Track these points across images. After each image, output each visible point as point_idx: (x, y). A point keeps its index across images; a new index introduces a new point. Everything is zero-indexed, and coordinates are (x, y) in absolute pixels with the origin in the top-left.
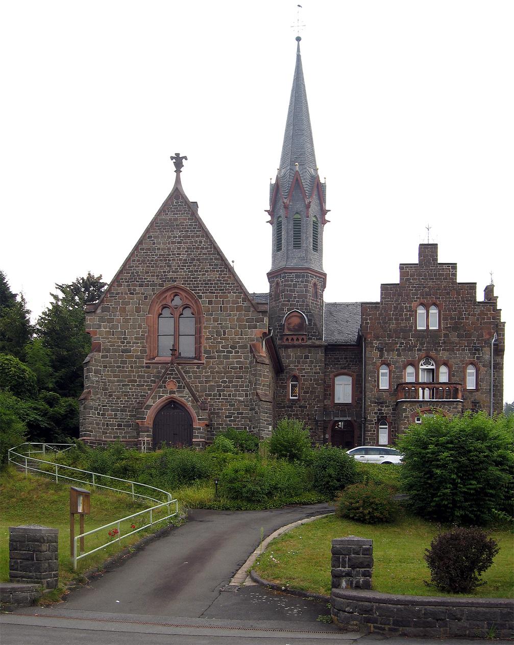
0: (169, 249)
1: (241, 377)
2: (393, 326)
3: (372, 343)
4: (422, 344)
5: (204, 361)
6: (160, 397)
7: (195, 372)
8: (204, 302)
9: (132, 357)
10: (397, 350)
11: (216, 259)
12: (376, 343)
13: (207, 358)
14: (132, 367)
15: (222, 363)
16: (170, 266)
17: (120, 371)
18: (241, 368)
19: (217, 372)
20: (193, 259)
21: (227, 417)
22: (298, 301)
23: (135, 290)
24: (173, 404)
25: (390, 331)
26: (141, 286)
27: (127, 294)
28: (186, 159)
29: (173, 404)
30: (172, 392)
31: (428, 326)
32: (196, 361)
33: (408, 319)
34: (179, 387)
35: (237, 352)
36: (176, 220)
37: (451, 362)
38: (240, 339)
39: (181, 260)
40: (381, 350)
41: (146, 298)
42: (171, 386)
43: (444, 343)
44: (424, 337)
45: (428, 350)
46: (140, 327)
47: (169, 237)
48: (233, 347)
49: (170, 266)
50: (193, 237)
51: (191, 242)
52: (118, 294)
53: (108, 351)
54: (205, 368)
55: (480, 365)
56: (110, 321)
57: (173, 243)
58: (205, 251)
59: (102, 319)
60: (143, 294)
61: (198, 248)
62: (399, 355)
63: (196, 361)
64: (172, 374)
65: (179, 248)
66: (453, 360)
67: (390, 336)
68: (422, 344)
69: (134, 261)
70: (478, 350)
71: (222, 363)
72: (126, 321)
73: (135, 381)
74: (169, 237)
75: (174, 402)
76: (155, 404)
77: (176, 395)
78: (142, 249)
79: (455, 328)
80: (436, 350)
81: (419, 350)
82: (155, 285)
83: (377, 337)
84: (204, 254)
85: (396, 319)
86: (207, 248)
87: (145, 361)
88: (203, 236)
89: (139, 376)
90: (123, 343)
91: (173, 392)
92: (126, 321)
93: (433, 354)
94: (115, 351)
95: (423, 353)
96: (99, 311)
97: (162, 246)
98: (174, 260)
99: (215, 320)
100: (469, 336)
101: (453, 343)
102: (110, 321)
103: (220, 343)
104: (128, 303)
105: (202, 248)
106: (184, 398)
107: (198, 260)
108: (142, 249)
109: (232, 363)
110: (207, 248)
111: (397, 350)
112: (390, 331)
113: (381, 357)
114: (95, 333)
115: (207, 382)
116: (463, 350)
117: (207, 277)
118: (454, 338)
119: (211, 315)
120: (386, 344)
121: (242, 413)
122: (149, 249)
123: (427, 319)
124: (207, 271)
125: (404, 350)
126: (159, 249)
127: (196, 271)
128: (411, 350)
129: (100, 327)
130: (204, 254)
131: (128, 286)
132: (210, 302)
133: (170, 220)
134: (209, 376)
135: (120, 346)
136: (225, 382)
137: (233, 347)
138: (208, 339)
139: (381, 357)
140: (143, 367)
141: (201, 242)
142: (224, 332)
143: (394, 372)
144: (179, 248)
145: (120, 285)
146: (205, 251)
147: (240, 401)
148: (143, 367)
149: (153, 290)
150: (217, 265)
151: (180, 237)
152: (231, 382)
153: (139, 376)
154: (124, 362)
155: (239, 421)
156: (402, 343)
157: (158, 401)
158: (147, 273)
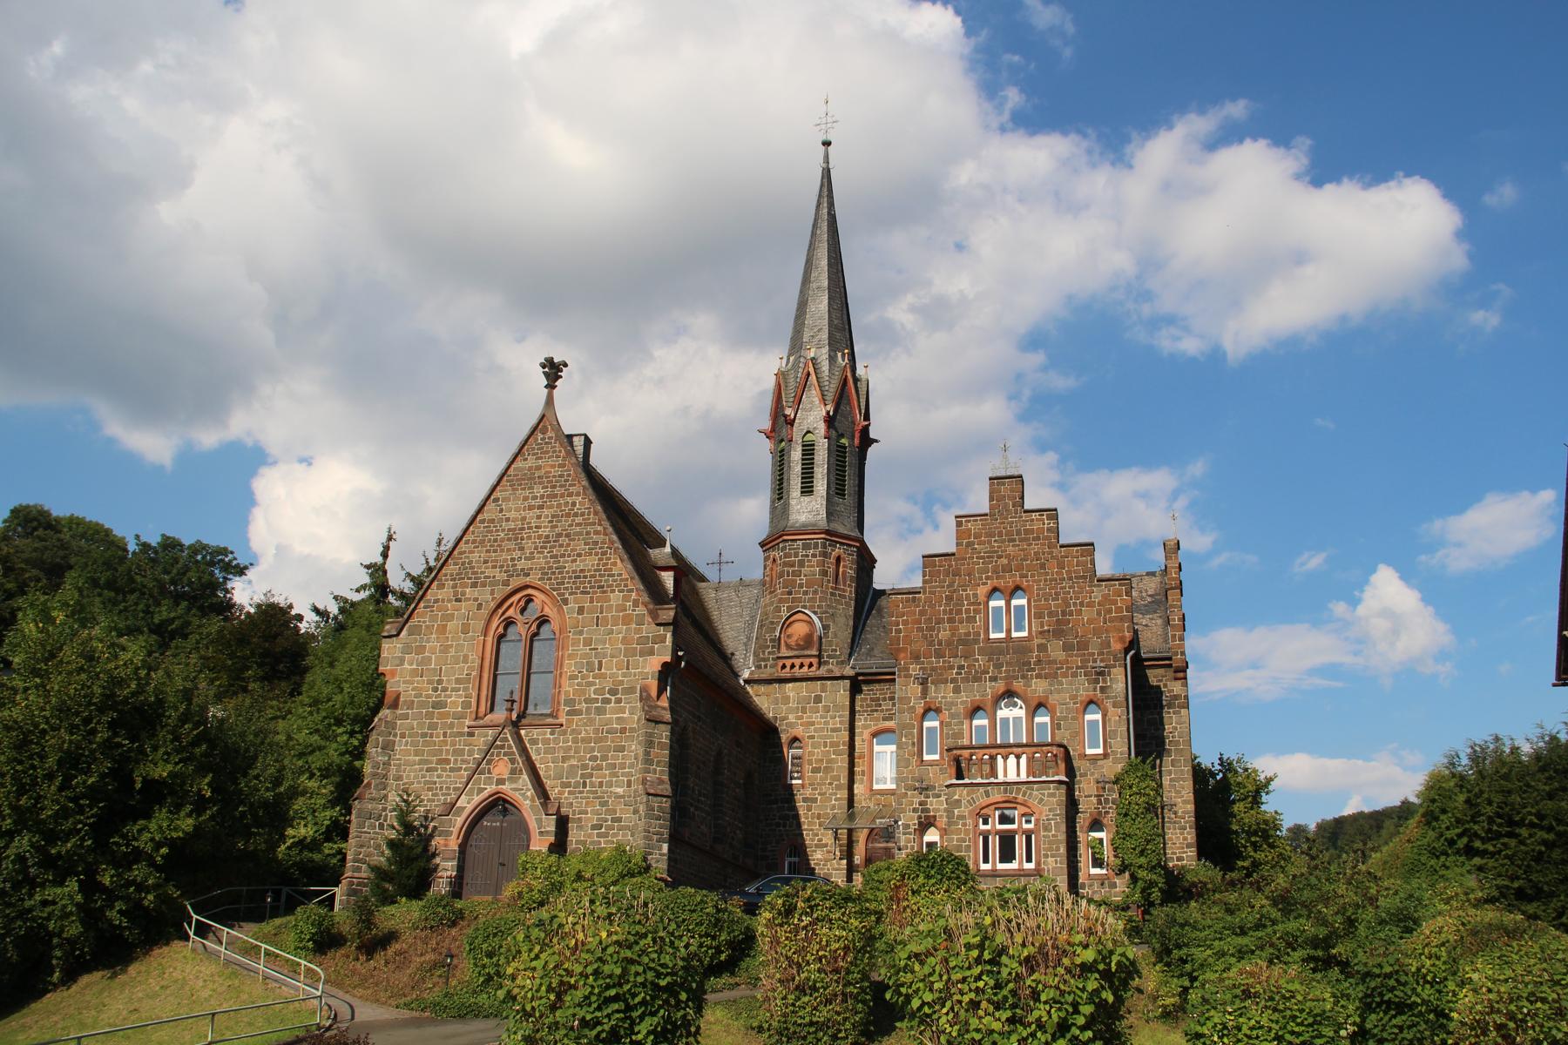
0: (524, 519)
1: (622, 749)
2: (944, 634)
3: (907, 669)
4: (998, 666)
5: (562, 720)
6: (481, 790)
7: (546, 741)
8: (571, 611)
9: (447, 715)
10: (953, 681)
11: (597, 533)
12: (914, 670)
13: (569, 713)
14: (445, 735)
15: (591, 722)
16: (522, 549)
17: (426, 744)
18: (623, 731)
19: (583, 740)
20: (559, 535)
21: (594, 827)
22: (806, 593)
23: (464, 594)
24: (498, 805)
25: (940, 644)
26: (474, 585)
27: (450, 601)
28: (566, 365)
29: (498, 805)
30: (501, 782)
31: (1009, 631)
32: (550, 720)
33: (971, 620)
34: (513, 771)
35: (619, 701)
36: (539, 468)
37: (1053, 700)
38: (624, 675)
39: (540, 537)
40: (924, 682)
41: (480, 606)
42: (502, 768)
43: (1039, 662)
44: (1001, 652)
45: (1009, 679)
46: (465, 660)
47: (526, 499)
48: (613, 692)
49: (522, 549)
50: (562, 496)
51: (559, 506)
52: (436, 601)
53: (410, 705)
54: (565, 733)
55: (1108, 704)
56: (420, 650)
57: (531, 508)
58: (579, 520)
59: (407, 649)
60: (476, 600)
61: (568, 515)
62: (957, 690)
63: (550, 720)
64: (502, 747)
65: (539, 517)
66: (1056, 696)
67: (939, 655)
68: (998, 666)
69: (467, 542)
70: (1101, 673)
71: (591, 722)
72: (445, 649)
73: (447, 761)
74: (526, 499)
75: (505, 801)
76: (468, 804)
77: (506, 788)
78: (483, 521)
79: (1058, 633)
80: (1023, 677)
81: (993, 679)
82: (493, 584)
83: (916, 658)
84: (579, 525)
85: (951, 620)
86: (583, 514)
87: (467, 722)
88: (578, 494)
89: (456, 752)
90: (435, 690)
91: (501, 782)
92: (445, 649)
93: (1018, 685)
94: (422, 705)
95: (1000, 686)
96: (404, 633)
97: (512, 515)
98: (529, 538)
99: (588, 642)
100: (1083, 646)
101: (1054, 662)
102: (420, 650)
103: (591, 684)
104: (451, 617)
105: (576, 515)
106: (521, 792)
107: (568, 535)
108: (483, 521)
109: (610, 721)
110: (583, 514)
111: (953, 681)
112: (940, 644)
113: (925, 693)
114: (393, 673)
115: (564, 759)
116: (1074, 675)
117: (579, 565)
118: (1056, 651)
119: (581, 633)
120: (933, 669)
121: (619, 820)
122: (492, 521)
123: (1008, 619)
124: (579, 555)
125: (966, 680)
126: (508, 520)
127: (563, 556)
128: (977, 679)
129: (402, 661)
130: (579, 525)
131: (455, 586)
132: (581, 611)
133: (530, 468)
134: (570, 748)
135: (428, 696)
136: (594, 758)
137: (613, 692)
138: (572, 677)
139: (925, 693)
140: (462, 734)
141: (574, 504)
142: (600, 663)
143: (949, 724)
144: (539, 517)
145: (442, 586)
146: (579, 520)
147: (618, 797)
148: (462, 734)
149: (492, 593)
150: (596, 543)
151: (542, 497)
152: (605, 758)
153: (456, 752)
154: (433, 726)
155: (615, 835)
156: (961, 667)
157: (477, 799)
158: (486, 562)
